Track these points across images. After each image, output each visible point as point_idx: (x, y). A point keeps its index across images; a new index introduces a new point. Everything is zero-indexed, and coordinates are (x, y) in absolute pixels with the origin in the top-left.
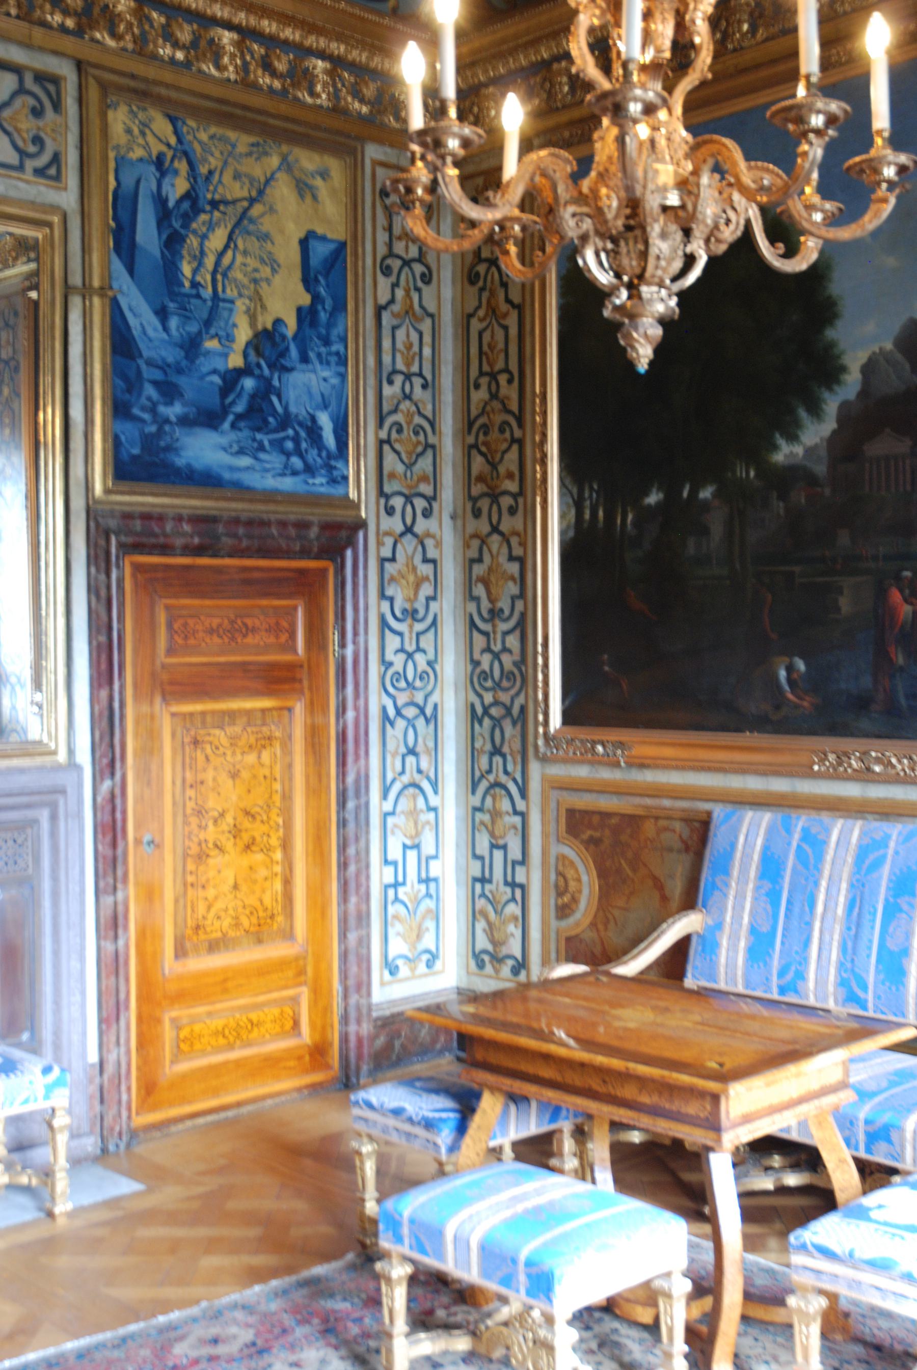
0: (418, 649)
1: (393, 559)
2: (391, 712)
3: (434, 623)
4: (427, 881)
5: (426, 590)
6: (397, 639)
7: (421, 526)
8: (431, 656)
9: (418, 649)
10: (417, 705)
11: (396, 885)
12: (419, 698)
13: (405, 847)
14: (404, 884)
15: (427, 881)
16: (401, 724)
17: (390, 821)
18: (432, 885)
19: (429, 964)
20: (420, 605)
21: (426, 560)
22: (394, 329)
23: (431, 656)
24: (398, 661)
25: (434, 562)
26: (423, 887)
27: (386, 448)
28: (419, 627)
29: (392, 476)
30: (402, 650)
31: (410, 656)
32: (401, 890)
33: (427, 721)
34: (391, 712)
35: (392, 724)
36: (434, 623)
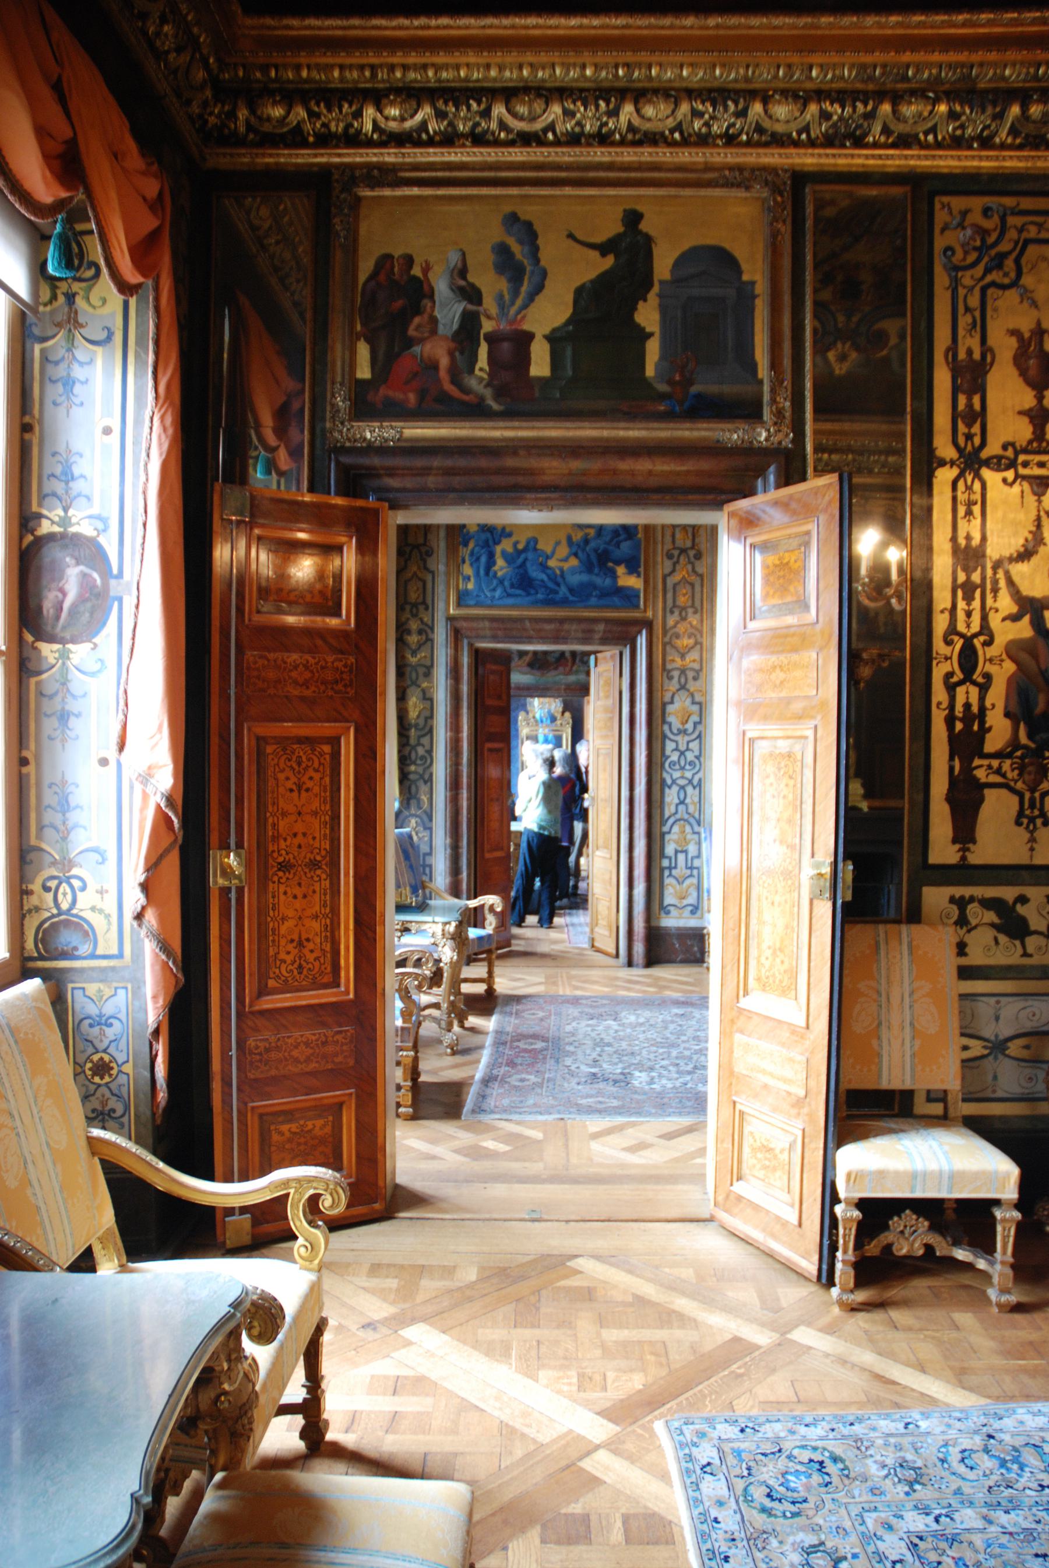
3: (699, 736)
4: (691, 868)
5: (695, 718)
7: (692, 686)
9: (688, 749)
11: (670, 868)
12: (688, 775)
15: (691, 868)
16: (675, 789)
18: (695, 872)
19: (693, 912)
20: (689, 726)
21: (693, 703)
23: (697, 753)
25: (700, 704)
26: (688, 872)
27: (668, 648)
28: (687, 738)
30: (676, 749)
31: (682, 753)
32: (674, 872)
36: (699, 736)
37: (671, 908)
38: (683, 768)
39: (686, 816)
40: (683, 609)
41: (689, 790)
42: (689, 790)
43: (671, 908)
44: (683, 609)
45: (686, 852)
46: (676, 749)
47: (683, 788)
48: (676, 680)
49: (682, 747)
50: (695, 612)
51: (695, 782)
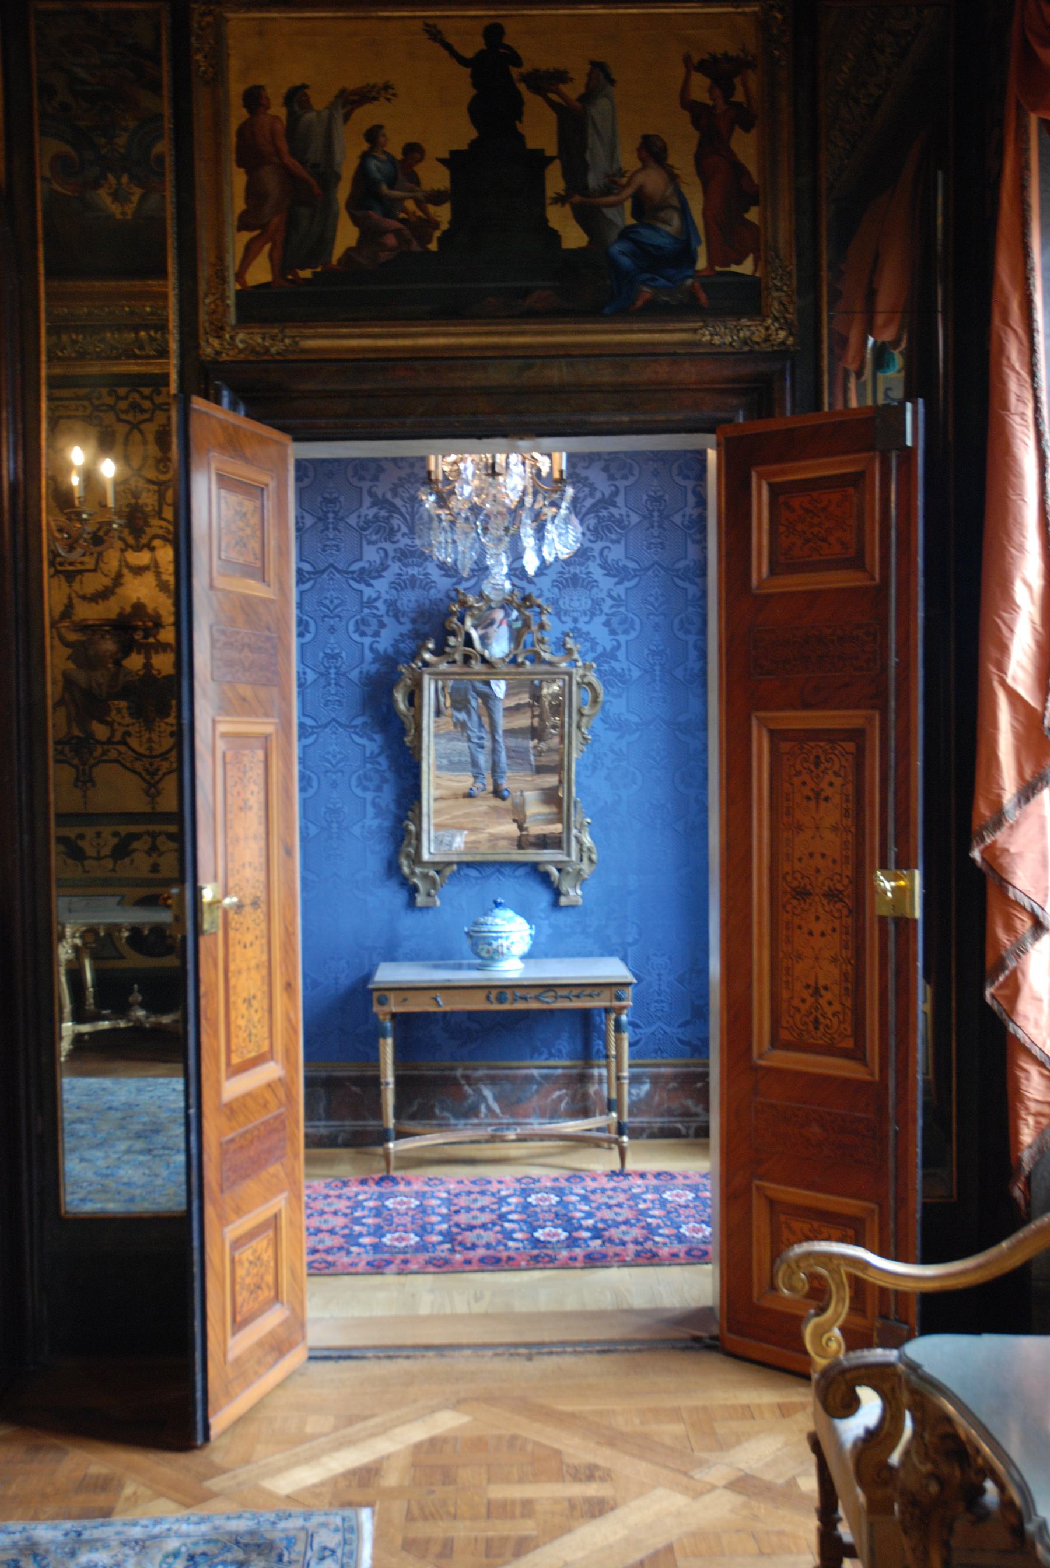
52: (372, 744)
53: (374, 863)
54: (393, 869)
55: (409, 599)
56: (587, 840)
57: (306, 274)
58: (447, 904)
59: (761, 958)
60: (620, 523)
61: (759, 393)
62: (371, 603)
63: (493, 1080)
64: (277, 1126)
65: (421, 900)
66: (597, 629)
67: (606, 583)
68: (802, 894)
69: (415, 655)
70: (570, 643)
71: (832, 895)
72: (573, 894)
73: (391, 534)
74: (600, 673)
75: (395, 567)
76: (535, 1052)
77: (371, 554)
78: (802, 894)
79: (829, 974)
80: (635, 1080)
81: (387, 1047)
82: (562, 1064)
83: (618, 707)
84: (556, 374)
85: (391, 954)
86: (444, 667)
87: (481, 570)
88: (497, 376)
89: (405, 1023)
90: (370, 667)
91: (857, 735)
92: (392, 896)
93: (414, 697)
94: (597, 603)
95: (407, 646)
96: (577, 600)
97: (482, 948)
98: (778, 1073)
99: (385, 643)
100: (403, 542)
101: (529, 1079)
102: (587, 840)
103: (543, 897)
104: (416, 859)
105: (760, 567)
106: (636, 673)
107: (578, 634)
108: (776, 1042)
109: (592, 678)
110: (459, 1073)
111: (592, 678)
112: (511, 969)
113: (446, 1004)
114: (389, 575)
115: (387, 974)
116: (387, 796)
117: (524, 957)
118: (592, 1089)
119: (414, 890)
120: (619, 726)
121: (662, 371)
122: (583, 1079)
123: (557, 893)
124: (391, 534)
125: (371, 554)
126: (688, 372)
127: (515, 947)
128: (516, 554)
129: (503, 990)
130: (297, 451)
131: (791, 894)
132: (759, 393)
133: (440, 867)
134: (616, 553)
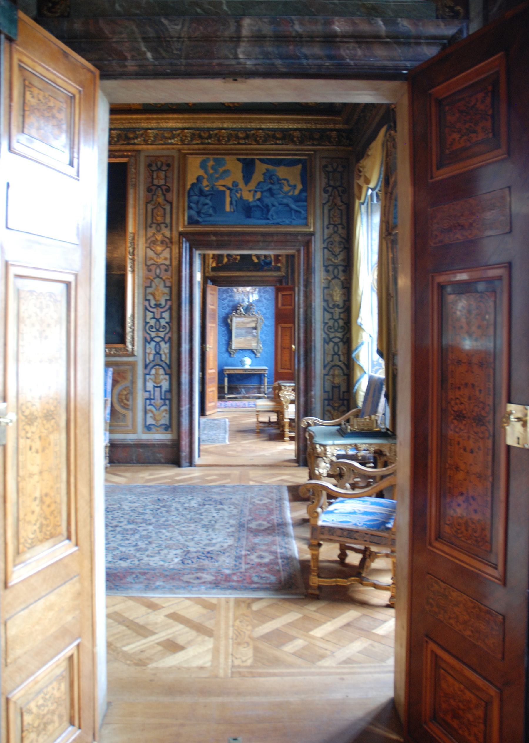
0: (162, 318)
1: (150, 287)
2: (149, 339)
6: (152, 314)
8: (168, 320)
9: (162, 318)
10: (160, 337)
12: (162, 334)
13: (155, 387)
14: (153, 399)
17: (148, 377)
22: (153, 210)
23: (168, 320)
24: (153, 322)
29: (151, 259)
31: (158, 320)
32: (153, 401)
33: (166, 343)
34: (149, 339)
35: (149, 343)
37: (152, 426)
38: (158, 330)
39: (161, 363)
40: (159, 225)
41: (162, 344)
42: (162, 344)
43: (152, 426)
44: (159, 225)
45: (160, 387)
46: (154, 318)
47: (158, 343)
48: (153, 271)
49: (158, 316)
50: (166, 227)
51: (167, 339)
52: (224, 329)
53: (224, 349)
54: (227, 350)
55: (231, 304)
56: (261, 346)
57: (220, 265)
58: (236, 356)
59: (279, 357)
60: (267, 291)
61: (280, 281)
62: (224, 304)
63: (244, 388)
64: (214, 378)
65: (232, 356)
66: (263, 309)
67: (265, 301)
68: (284, 348)
69: (232, 313)
70: (259, 312)
71: (288, 348)
72: (259, 355)
73: (228, 292)
74: (264, 317)
75: (229, 298)
76: (251, 383)
77: (225, 296)
78: (284, 348)
79: (287, 359)
80: (268, 388)
81: (226, 380)
82: (256, 385)
83: (267, 323)
84: (253, 279)
85: (227, 365)
86: (237, 315)
87: (243, 301)
88: (246, 279)
89: (230, 376)
90: (224, 315)
91: (291, 327)
92: (226, 355)
93: (231, 321)
94: (263, 305)
95: (230, 312)
96: (260, 304)
97: (242, 364)
98: (282, 373)
99: (227, 311)
100: (230, 294)
101: (250, 388)
102: (261, 346)
103: (253, 355)
104: (231, 349)
105: (280, 305)
106: (270, 317)
107: (260, 310)
108: (282, 369)
109: (262, 318)
110: (238, 386)
111: (262, 318)
112: (247, 367)
113: (236, 372)
114: (227, 300)
115: (226, 367)
116: (226, 338)
117: (250, 366)
118: (262, 390)
119: (230, 354)
120: (266, 326)
121: (267, 278)
122: (260, 388)
123: (255, 355)
124: (228, 292)
125: (225, 296)
126: (271, 279)
127: (248, 363)
128: (249, 299)
129: (246, 370)
130: (218, 288)
131: (283, 348)
132: (280, 281)
133: (235, 350)
134: (267, 296)
